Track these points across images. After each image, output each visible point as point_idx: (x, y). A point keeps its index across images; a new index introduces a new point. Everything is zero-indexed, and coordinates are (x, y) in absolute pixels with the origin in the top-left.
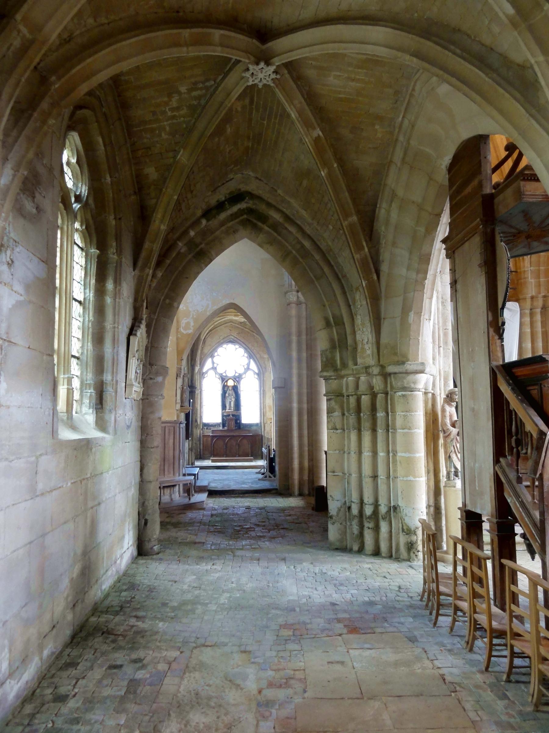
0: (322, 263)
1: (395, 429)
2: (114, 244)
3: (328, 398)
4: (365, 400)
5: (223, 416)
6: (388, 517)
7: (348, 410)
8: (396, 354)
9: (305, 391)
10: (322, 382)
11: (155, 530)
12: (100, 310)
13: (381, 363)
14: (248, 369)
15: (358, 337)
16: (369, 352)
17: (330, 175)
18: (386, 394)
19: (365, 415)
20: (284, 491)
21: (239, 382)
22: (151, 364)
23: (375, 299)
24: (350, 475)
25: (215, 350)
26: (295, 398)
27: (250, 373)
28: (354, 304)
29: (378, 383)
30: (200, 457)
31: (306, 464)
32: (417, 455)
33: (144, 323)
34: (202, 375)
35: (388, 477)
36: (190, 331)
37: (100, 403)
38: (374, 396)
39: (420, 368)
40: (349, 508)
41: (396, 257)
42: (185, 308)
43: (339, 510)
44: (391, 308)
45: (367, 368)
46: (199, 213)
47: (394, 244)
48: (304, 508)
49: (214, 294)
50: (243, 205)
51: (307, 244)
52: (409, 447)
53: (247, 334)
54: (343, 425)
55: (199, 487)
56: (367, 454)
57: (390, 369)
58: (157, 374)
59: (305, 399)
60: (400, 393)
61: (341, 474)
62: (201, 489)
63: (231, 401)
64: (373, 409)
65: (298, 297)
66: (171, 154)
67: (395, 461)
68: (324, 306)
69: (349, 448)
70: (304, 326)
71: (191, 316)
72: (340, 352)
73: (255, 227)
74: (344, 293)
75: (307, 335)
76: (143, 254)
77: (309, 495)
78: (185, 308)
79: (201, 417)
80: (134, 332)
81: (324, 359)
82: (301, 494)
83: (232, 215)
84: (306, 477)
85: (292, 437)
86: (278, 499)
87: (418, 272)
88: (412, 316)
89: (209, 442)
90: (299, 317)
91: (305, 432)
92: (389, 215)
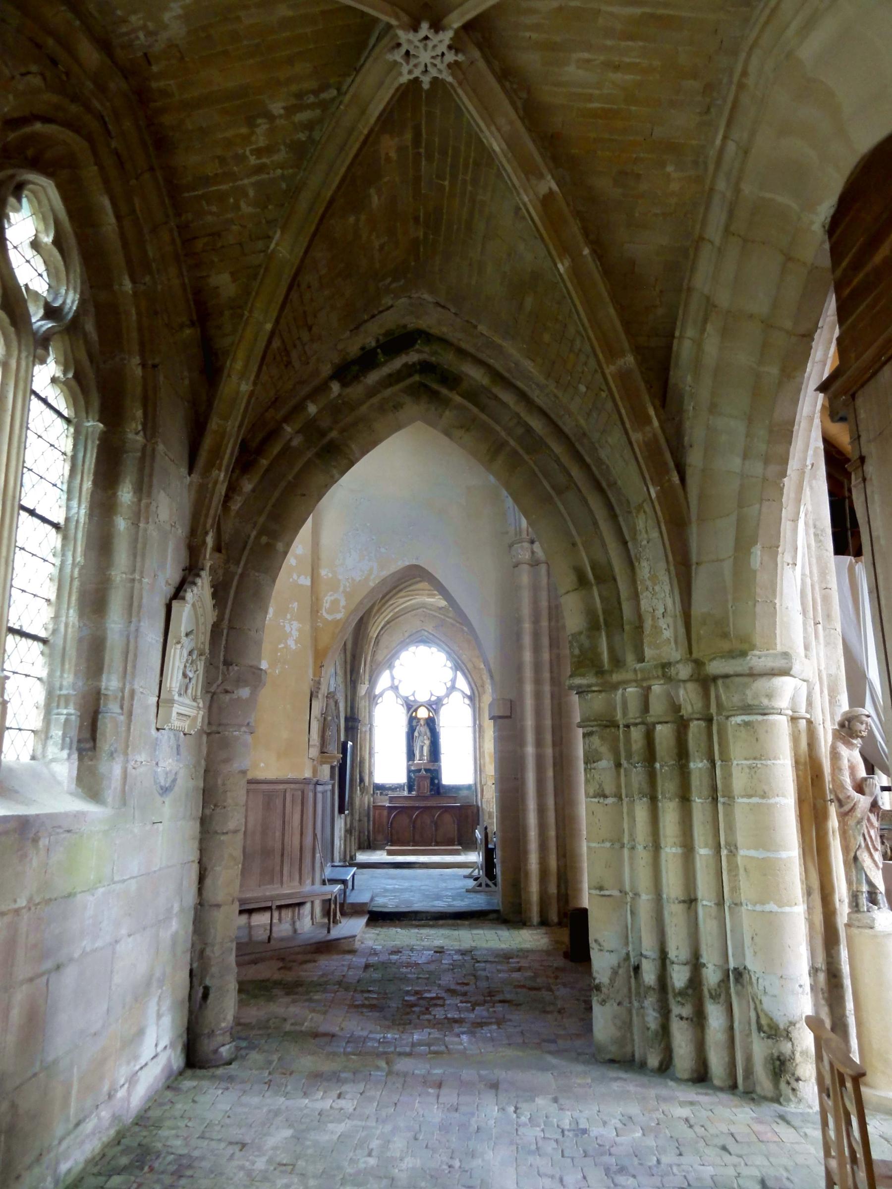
0: (565, 459)
1: (730, 797)
2: (139, 413)
3: (586, 730)
4: (664, 733)
5: (409, 771)
6: (722, 993)
7: (629, 757)
8: (725, 635)
9: (548, 722)
10: (575, 698)
11: (226, 1008)
12: (101, 544)
13: (695, 655)
14: (453, 688)
15: (644, 604)
16: (668, 634)
17: (577, 272)
18: (709, 720)
19: (664, 766)
20: (510, 916)
21: (436, 711)
22: (227, 663)
23: (677, 525)
24: (637, 895)
25: (395, 655)
26: (530, 737)
27: (456, 696)
28: (634, 539)
29: (689, 698)
30: (368, 845)
31: (553, 863)
32: (784, 855)
33: (205, 574)
34: (373, 699)
35: (720, 903)
36: (339, 616)
37: (89, 734)
38: (682, 726)
39: (779, 663)
40: (637, 969)
41: (718, 435)
42: (330, 575)
43: (615, 973)
44: (712, 542)
45: (665, 666)
46: (326, 370)
47: (713, 408)
48: (548, 953)
49: (383, 550)
50: (412, 357)
51: (537, 424)
52: (765, 836)
53: (452, 630)
54: (619, 787)
55: (353, 904)
56: (671, 851)
57: (715, 667)
58: (239, 682)
59: (548, 738)
60: (739, 719)
61: (616, 893)
62: (356, 910)
63: (423, 744)
64: (682, 754)
65: (533, 552)
66: (260, 244)
67: (733, 868)
68: (574, 545)
69: (632, 838)
70: (544, 604)
71: (341, 589)
72: (608, 637)
73: (434, 395)
74: (613, 516)
75: (550, 620)
76: (208, 442)
77: (560, 924)
78: (330, 575)
79: (371, 774)
80: (181, 594)
81: (577, 652)
82: (544, 922)
83: (390, 375)
84: (553, 889)
85: (524, 810)
86: (500, 932)
87: (767, 461)
88: (757, 554)
89: (385, 820)
90: (535, 588)
91: (551, 802)
92: (701, 350)
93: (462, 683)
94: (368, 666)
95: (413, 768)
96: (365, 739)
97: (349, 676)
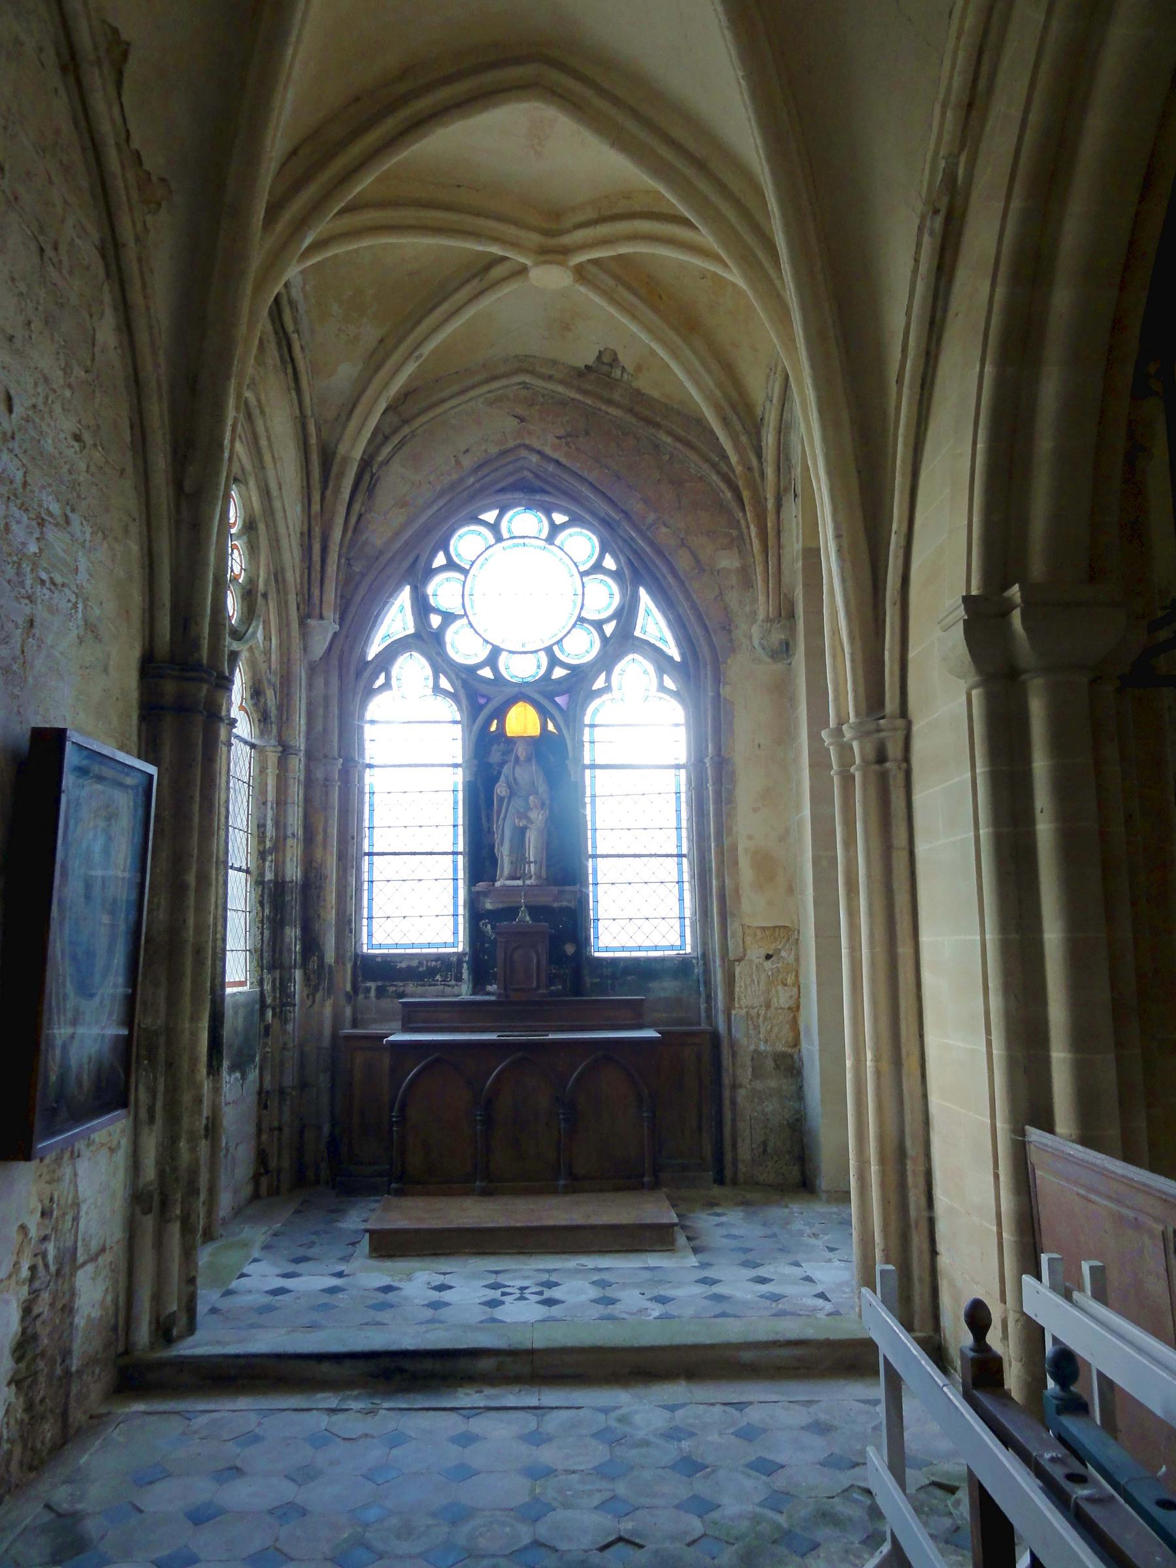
5: (476, 915)
14: (621, 639)
21: (572, 718)
79: (347, 925)
93: (653, 623)
94: (333, 556)
95: (489, 906)
96: (326, 808)
97: (161, 462)
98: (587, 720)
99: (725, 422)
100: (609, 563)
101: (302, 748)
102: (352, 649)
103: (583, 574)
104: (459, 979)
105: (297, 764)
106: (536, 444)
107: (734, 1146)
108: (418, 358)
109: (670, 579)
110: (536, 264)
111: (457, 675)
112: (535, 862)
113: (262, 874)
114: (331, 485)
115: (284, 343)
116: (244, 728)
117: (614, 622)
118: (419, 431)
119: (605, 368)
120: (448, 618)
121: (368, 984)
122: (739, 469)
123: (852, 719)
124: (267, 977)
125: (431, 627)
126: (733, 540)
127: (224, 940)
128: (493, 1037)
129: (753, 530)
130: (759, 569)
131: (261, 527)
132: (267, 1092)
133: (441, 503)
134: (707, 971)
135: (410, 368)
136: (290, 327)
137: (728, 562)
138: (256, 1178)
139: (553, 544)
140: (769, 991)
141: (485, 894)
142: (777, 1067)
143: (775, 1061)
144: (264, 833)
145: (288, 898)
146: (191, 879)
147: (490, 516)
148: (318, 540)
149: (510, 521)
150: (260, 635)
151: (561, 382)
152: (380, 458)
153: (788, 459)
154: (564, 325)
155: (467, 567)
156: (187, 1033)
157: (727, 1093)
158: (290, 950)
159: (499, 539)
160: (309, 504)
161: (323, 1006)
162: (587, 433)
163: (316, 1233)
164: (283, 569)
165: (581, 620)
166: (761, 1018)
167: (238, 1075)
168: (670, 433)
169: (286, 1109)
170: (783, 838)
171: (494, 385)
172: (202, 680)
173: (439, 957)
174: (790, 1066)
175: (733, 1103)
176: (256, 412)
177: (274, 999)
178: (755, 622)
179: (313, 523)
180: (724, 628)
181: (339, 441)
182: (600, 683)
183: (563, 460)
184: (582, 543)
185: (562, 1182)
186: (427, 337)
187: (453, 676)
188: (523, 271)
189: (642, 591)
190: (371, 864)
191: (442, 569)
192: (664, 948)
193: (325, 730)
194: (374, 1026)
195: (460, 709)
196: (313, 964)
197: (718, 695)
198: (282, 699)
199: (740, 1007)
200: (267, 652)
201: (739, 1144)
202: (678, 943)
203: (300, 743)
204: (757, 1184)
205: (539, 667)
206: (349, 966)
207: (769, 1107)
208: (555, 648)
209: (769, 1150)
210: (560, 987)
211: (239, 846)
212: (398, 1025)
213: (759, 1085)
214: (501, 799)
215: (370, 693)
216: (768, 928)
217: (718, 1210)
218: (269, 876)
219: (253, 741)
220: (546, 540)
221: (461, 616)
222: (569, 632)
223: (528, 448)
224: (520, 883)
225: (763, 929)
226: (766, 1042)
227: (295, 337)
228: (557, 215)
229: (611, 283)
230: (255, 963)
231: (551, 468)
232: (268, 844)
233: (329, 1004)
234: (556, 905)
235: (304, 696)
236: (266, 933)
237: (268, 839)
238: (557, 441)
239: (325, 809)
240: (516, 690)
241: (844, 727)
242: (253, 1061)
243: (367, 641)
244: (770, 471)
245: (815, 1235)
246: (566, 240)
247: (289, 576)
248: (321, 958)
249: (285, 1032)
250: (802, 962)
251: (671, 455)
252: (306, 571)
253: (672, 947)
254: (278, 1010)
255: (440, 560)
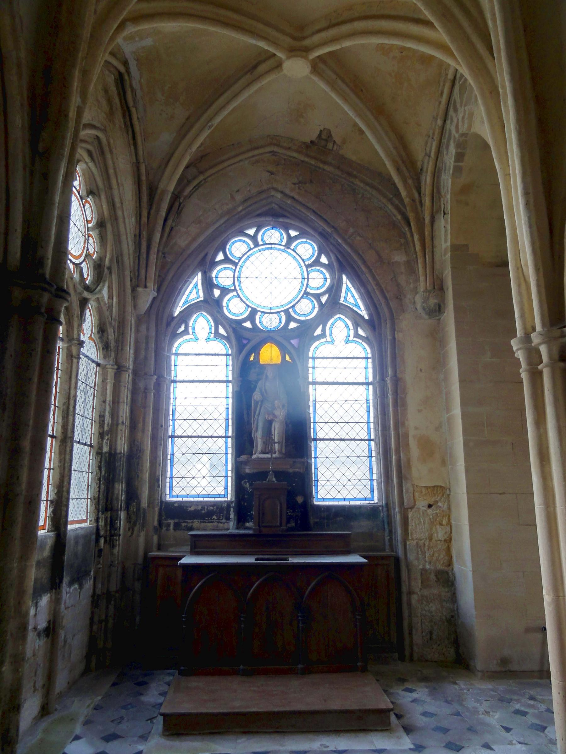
5: (239, 477)
14: (332, 305)
79: (156, 482)
93: (351, 295)
94: (154, 249)
95: (247, 471)
96: (145, 407)
98: (310, 355)
99: (398, 169)
100: (324, 259)
101: (131, 367)
102: (164, 308)
103: (308, 266)
104: (228, 518)
105: (127, 378)
106: (280, 187)
107: (410, 634)
108: (210, 127)
109: (363, 268)
110: (288, 58)
111: (230, 326)
112: (278, 443)
113: (101, 448)
114: (154, 207)
115: (127, 114)
116: (90, 349)
117: (327, 295)
118: (209, 179)
119: (323, 143)
120: (225, 291)
121: (169, 521)
122: (407, 200)
123: (539, 327)
124: (101, 516)
125: (214, 296)
126: (401, 245)
127: (68, 492)
128: (250, 560)
129: (416, 237)
130: (420, 261)
131: (109, 226)
132: (98, 596)
133: (222, 221)
134: (389, 516)
135: (206, 133)
136: (131, 103)
137: (399, 258)
138: (88, 657)
139: (289, 248)
140: (431, 529)
141: (246, 463)
142: (438, 580)
143: (436, 576)
144: (103, 421)
145: (118, 464)
146: (26, 444)
147: (251, 232)
148: (145, 239)
149: (263, 234)
150: (105, 292)
151: (297, 151)
152: (186, 193)
153: (439, 192)
154: (299, 113)
155: (237, 261)
156: (15, 571)
157: (405, 598)
158: (117, 498)
159: (256, 245)
160: (140, 218)
161: (138, 536)
162: (311, 182)
163: (125, 707)
164: (122, 255)
165: (306, 294)
166: (426, 548)
167: (76, 586)
168: (363, 181)
169: (111, 608)
170: (438, 428)
171: (256, 152)
172: (45, 290)
173: (215, 504)
174: (446, 579)
175: (409, 604)
176: (106, 149)
177: (106, 531)
178: (416, 293)
179: (142, 229)
180: (397, 298)
181: (159, 181)
182: (318, 331)
183: (296, 197)
184: (307, 249)
185: (300, 666)
186: (216, 114)
187: (228, 327)
188: (279, 65)
189: (344, 277)
190: (173, 443)
191: (221, 262)
192: (360, 499)
193: (146, 358)
194: (172, 549)
195: (231, 347)
196: (133, 509)
197: (394, 338)
198: (118, 336)
199: (413, 539)
200: (110, 307)
201: (414, 632)
202: (369, 496)
203: (130, 364)
204: (427, 661)
205: (280, 321)
206: (157, 509)
207: (434, 607)
208: (291, 310)
209: (434, 637)
210: (293, 524)
211: (84, 429)
212: (188, 548)
213: (426, 592)
214: (257, 403)
215: (175, 336)
216: (430, 487)
217: (409, 686)
218: (105, 449)
219: (99, 361)
220: (285, 246)
221: (233, 291)
222: (299, 301)
223: (276, 190)
224: (269, 456)
225: (427, 487)
226: (430, 563)
227: (133, 110)
228: (302, 28)
229: (334, 77)
230: (93, 507)
231: (289, 202)
232: (106, 428)
233: (143, 534)
234: (291, 471)
235: (133, 335)
236: (102, 487)
237: (106, 425)
238: (293, 186)
239: (145, 407)
240: (266, 334)
241: (533, 335)
242: (90, 575)
243: (174, 305)
244: (427, 201)
245: (487, 713)
246: (307, 42)
247: (126, 258)
248: (139, 504)
249: (112, 554)
250: (453, 509)
251: (363, 195)
252: (137, 259)
253: (365, 499)
254: (108, 539)
255: (220, 257)
